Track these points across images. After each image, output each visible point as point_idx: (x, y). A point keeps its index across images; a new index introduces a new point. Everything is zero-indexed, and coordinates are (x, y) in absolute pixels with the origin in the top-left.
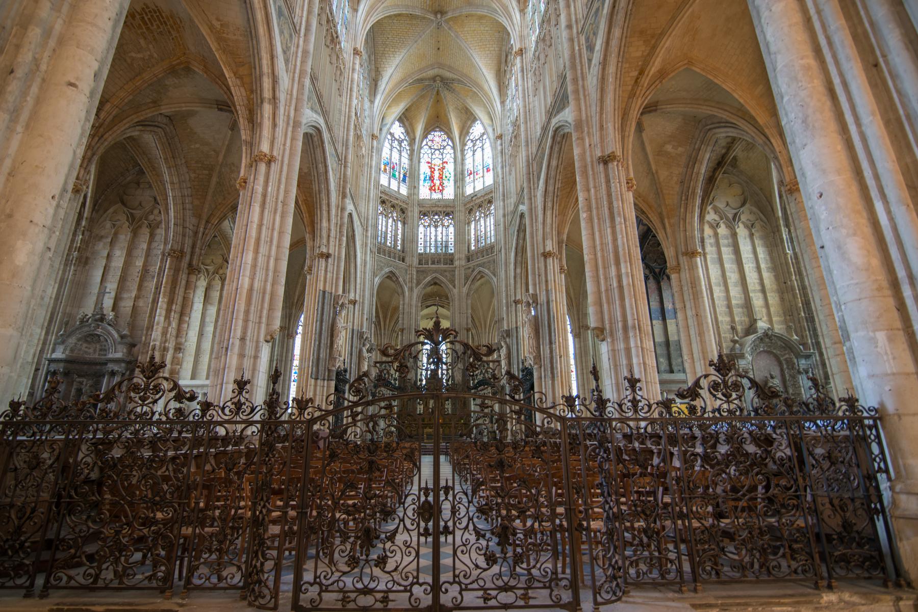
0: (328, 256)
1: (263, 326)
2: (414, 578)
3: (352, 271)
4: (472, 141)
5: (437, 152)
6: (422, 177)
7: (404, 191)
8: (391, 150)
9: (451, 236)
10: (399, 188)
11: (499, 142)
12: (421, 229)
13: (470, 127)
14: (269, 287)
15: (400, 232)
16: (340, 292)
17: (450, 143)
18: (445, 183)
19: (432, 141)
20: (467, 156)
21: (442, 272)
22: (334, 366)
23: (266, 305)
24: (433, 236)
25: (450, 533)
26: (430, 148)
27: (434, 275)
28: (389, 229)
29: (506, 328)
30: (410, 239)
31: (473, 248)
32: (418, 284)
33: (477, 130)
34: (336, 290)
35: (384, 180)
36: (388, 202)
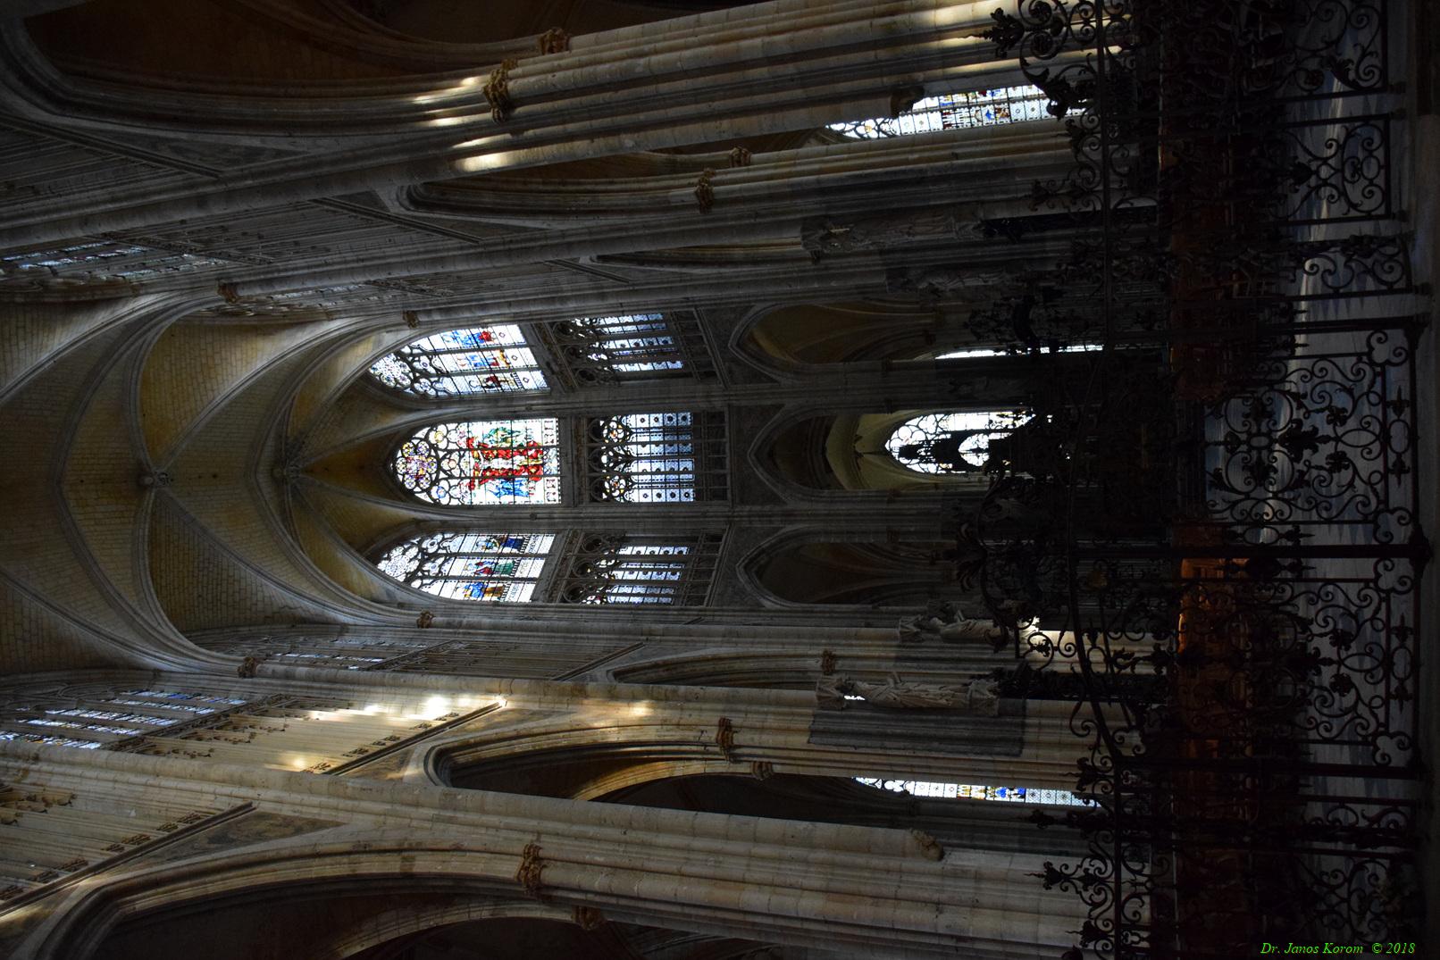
0: (725, 726)
1: (908, 864)
2: (1367, 587)
3: (751, 665)
4: (416, 380)
5: (445, 464)
6: (507, 499)
7: (544, 544)
8: (447, 578)
9: (651, 420)
10: (537, 556)
11: (423, 318)
12: (636, 496)
13: (382, 387)
14: (821, 855)
15: (643, 550)
16: (811, 694)
17: (421, 434)
18: (520, 440)
19: (418, 478)
22: (990, 703)
23: (861, 860)
24: (649, 466)
25: (1298, 529)
26: (435, 482)
27: (751, 459)
28: (641, 576)
29: (882, 280)
31: (679, 365)
32: (774, 499)
33: (390, 370)
34: (808, 704)
35: (522, 594)
36: (572, 578)
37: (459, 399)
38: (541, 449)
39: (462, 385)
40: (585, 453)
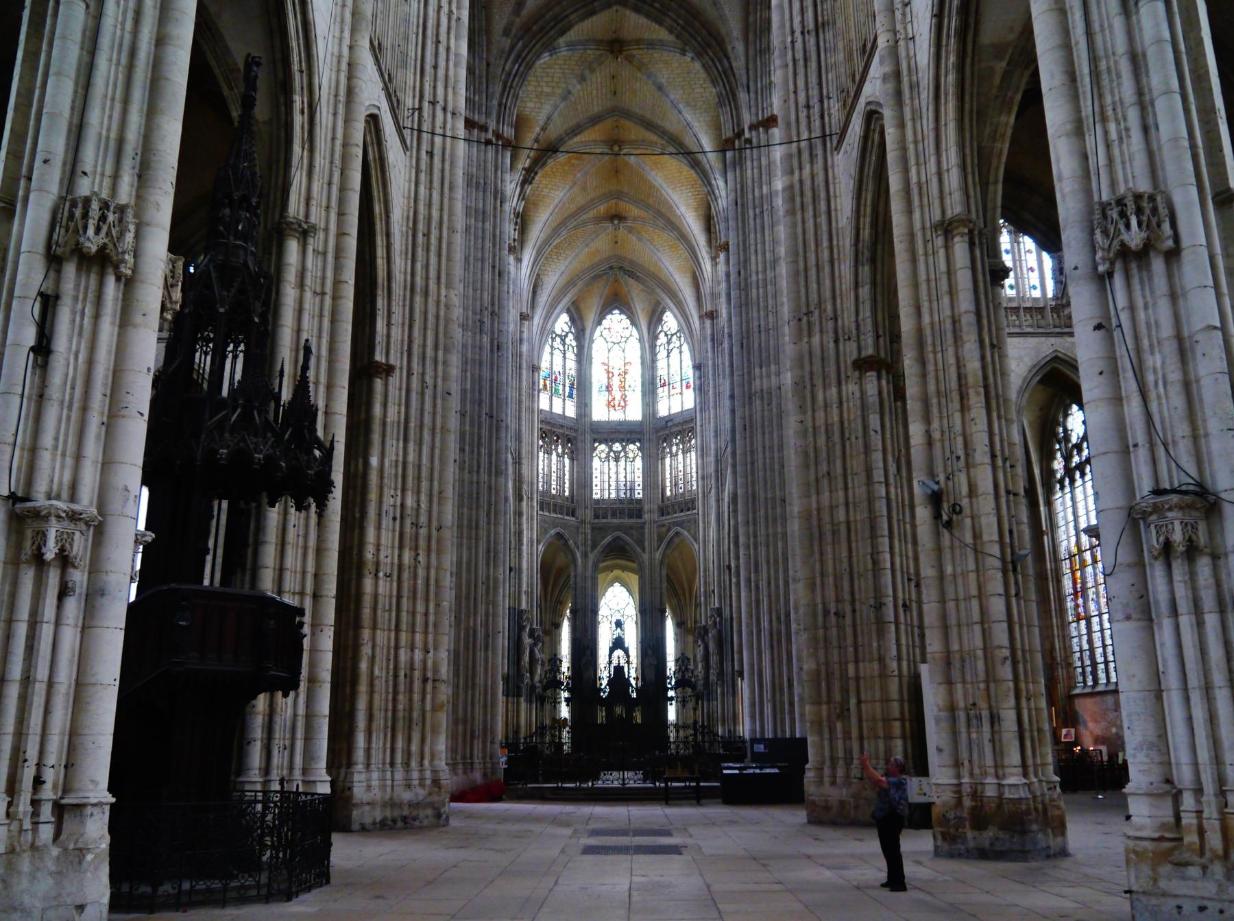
7: (571, 411)
8: (552, 354)
12: (596, 463)
20: (659, 357)
21: (627, 529)
27: (615, 534)
30: (583, 480)
31: (668, 493)
32: (594, 547)
37: (654, 361)
38: (624, 407)
39: (661, 364)
40: (622, 436)
